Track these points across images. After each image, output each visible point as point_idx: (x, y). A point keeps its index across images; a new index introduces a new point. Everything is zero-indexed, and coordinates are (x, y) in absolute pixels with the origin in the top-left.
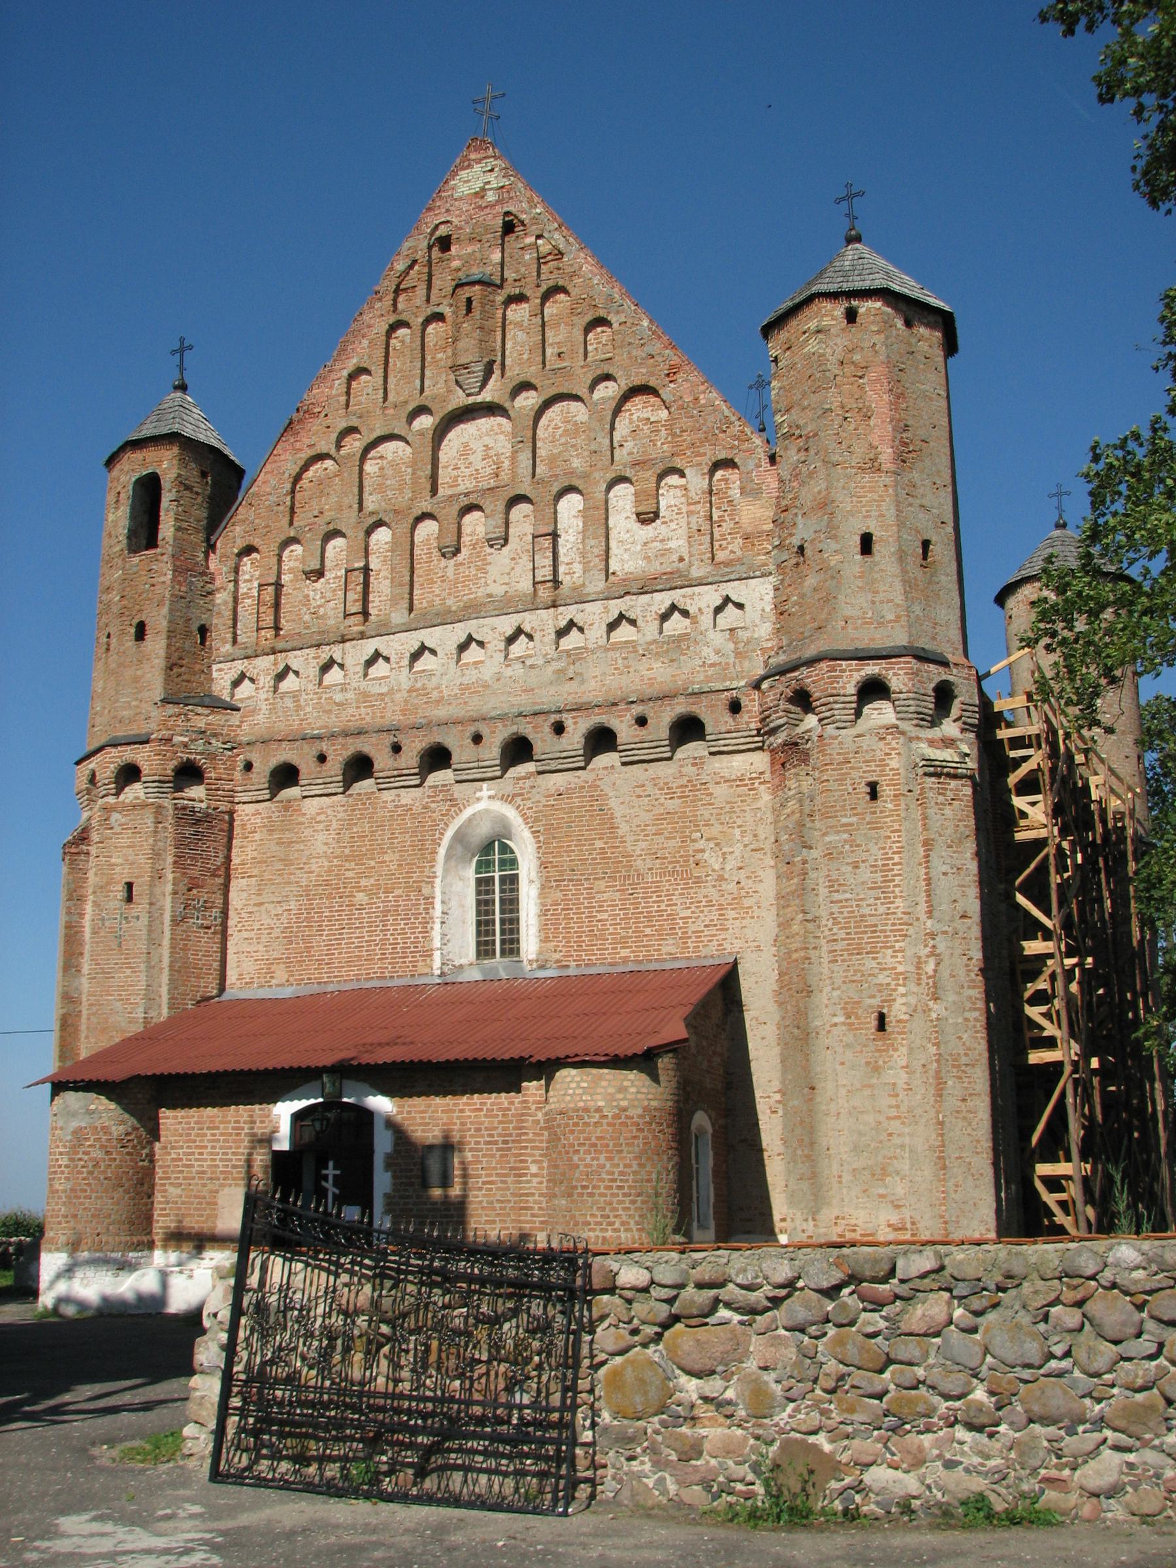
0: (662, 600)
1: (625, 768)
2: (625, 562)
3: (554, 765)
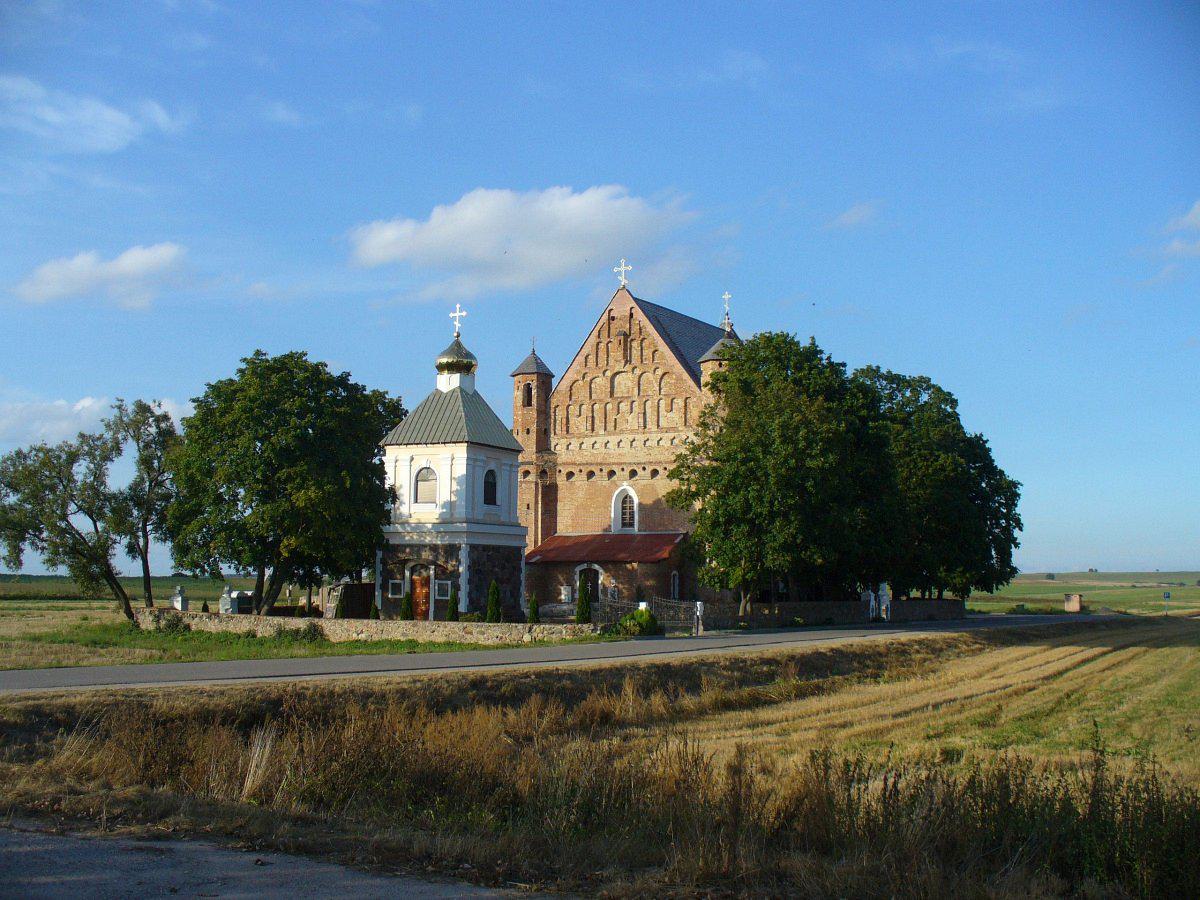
2: (663, 423)
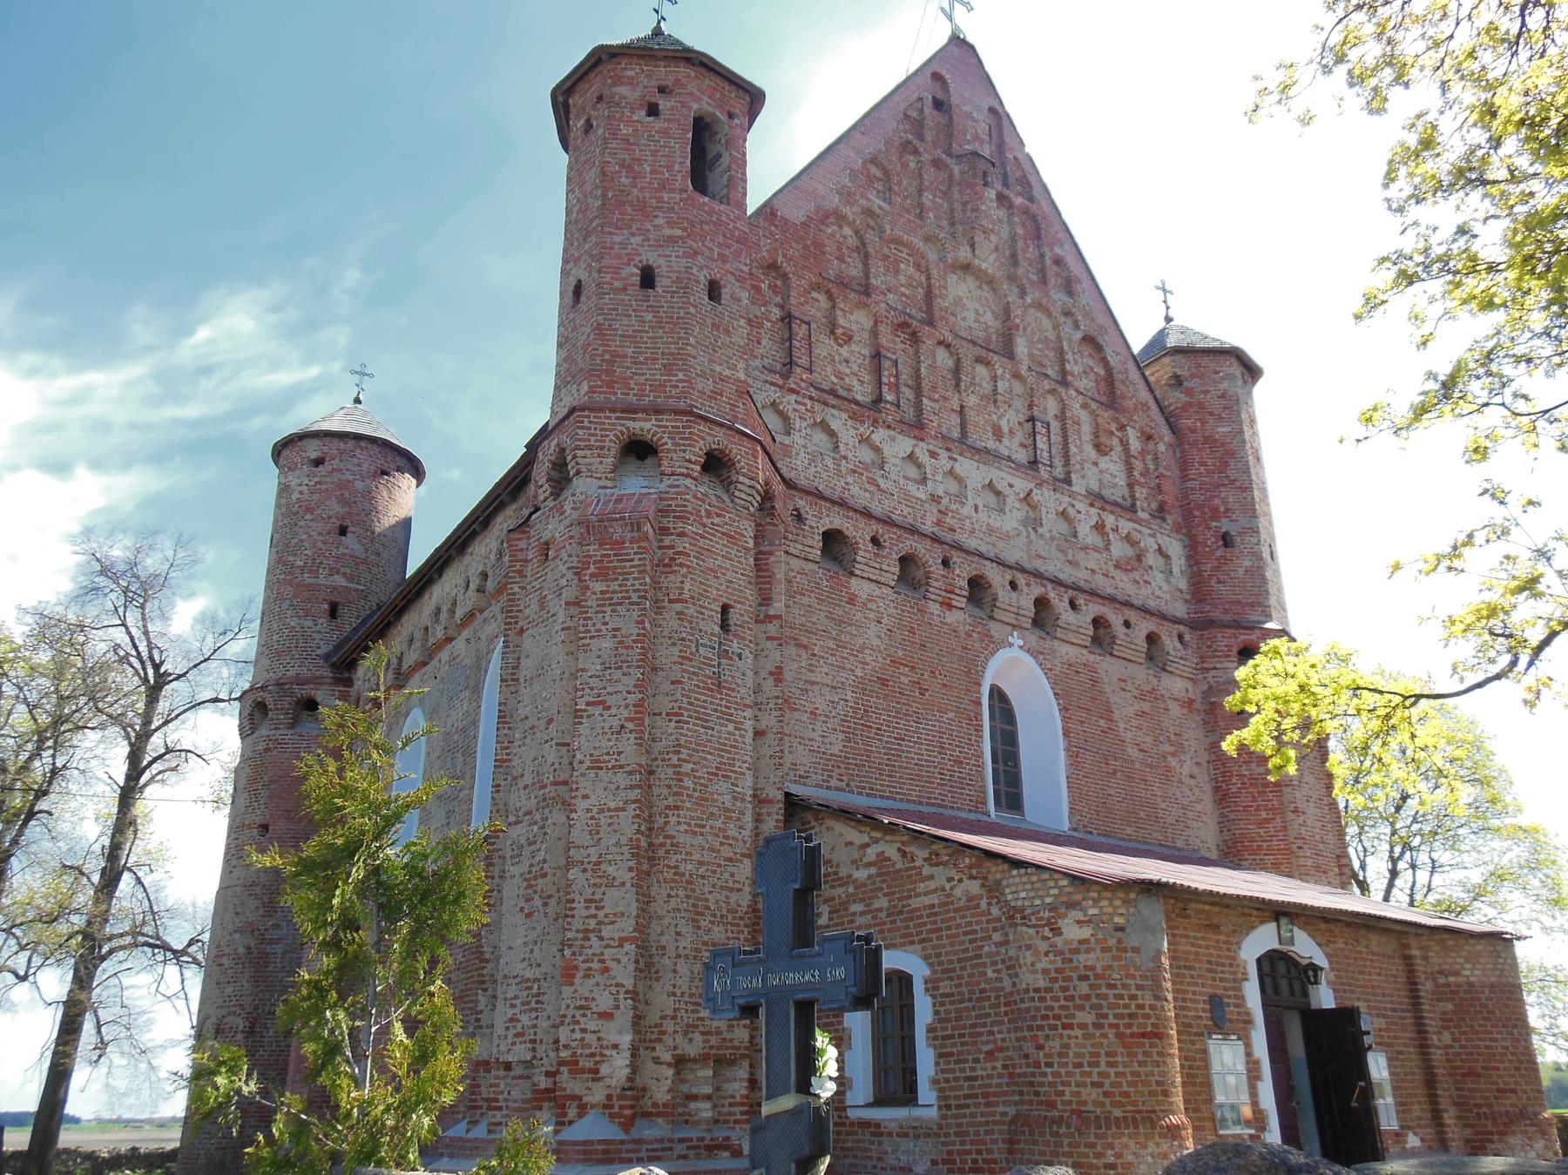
0: (1126, 526)
1: (1113, 660)
3: (1071, 637)
